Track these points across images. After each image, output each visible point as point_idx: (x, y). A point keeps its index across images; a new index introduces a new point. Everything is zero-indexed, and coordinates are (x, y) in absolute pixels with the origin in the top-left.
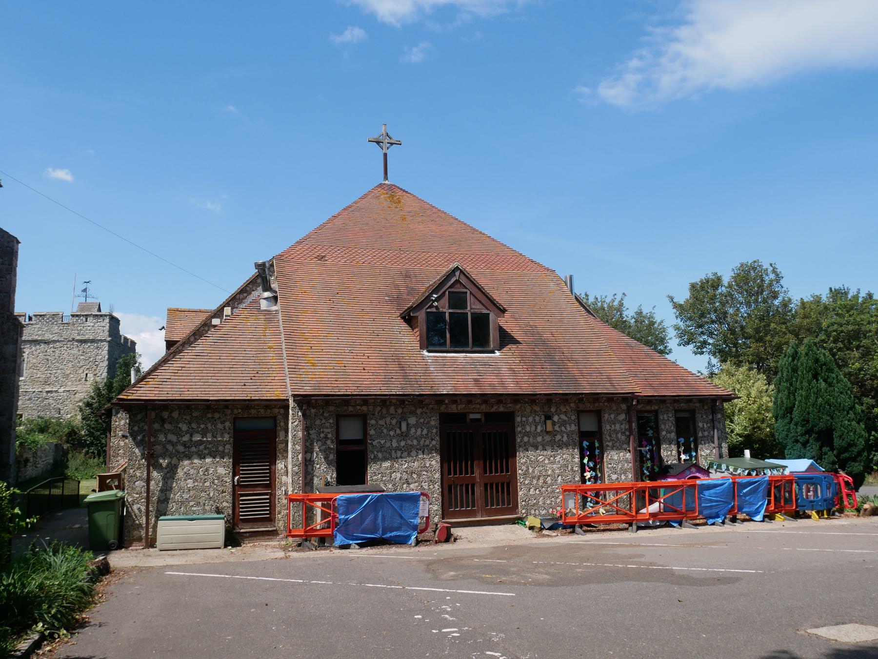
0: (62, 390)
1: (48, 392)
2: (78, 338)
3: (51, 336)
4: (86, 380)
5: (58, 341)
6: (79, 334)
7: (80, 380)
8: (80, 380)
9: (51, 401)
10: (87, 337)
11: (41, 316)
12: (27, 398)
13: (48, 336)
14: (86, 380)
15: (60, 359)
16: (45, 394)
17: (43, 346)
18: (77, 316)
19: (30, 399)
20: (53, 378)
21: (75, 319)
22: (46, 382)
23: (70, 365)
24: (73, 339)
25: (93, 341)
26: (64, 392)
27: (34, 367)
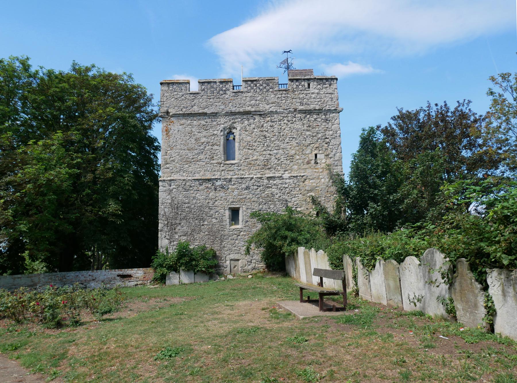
0: (286, 175)
1: (269, 178)
2: (301, 108)
3: (267, 107)
4: (316, 163)
5: (276, 113)
6: (301, 104)
7: (308, 163)
8: (308, 163)
9: (274, 190)
10: (312, 107)
11: (252, 81)
12: (244, 186)
13: (264, 107)
14: (316, 163)
15: (281, 136)
16: (266, 181)
17: (257, 118)
18: (297, 80)
19: (247, 188)
20: (274, 161)
21: (295, 85)
22: (266, 166)
23: (294, 143)
24: (295, 110)
25: (319, 112)
26: (290, 178)
27: (249, 146)
